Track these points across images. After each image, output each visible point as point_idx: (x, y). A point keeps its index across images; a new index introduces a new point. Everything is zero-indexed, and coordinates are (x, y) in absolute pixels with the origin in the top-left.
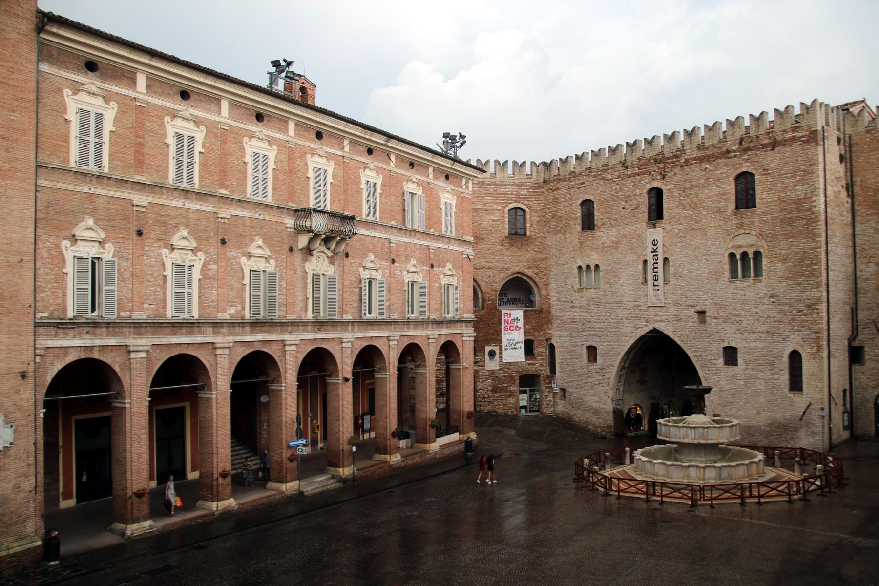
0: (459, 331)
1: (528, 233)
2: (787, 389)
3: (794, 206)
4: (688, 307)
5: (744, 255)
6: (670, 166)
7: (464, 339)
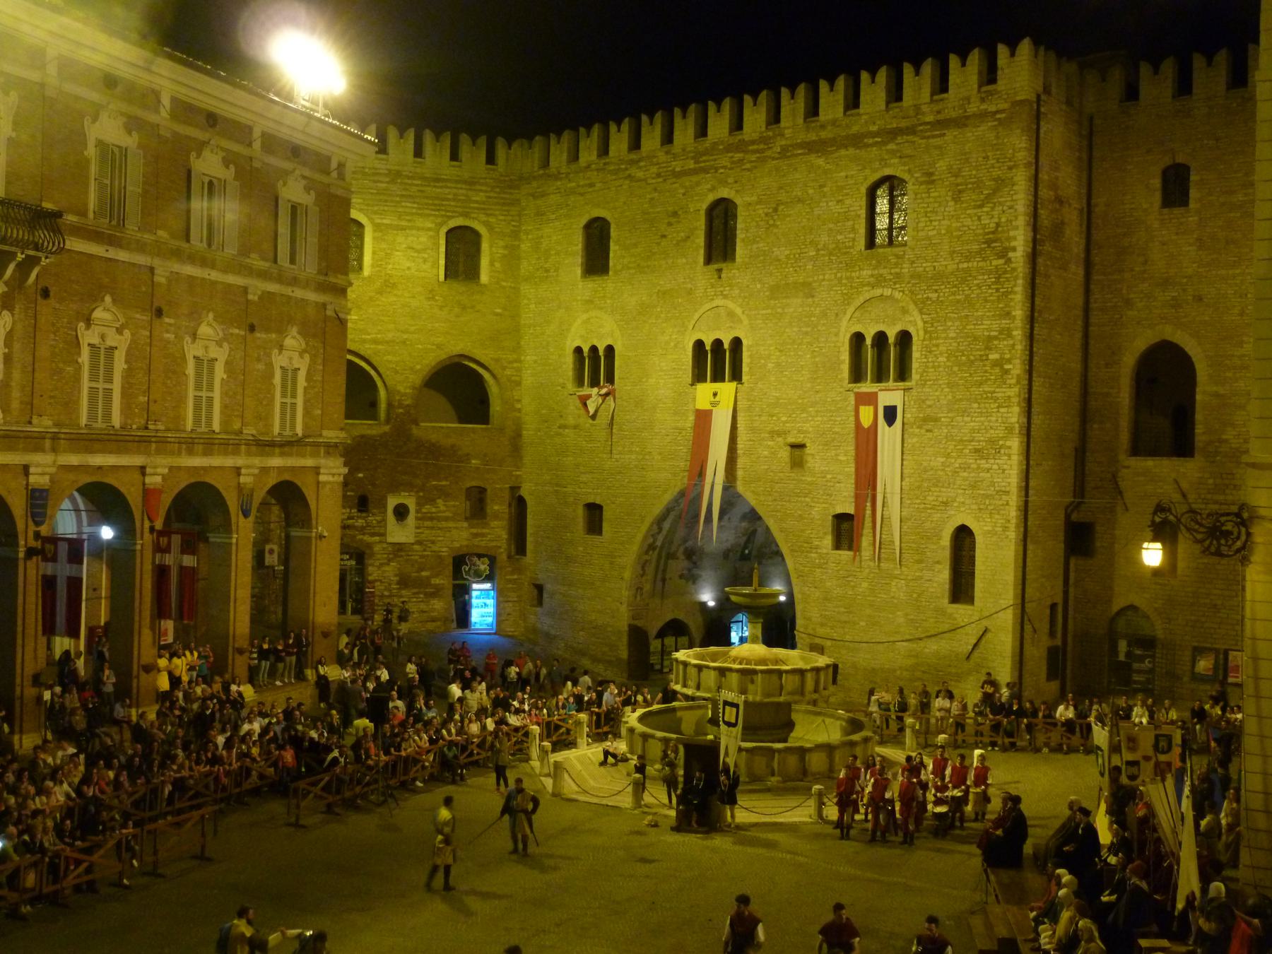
0: (309, 462)
1: (484, 278)
2: (946, 601)
3: (975, 247)
4: (774, 434)
5: (881, 338)
6: (753, 157)
7: (322, 478)
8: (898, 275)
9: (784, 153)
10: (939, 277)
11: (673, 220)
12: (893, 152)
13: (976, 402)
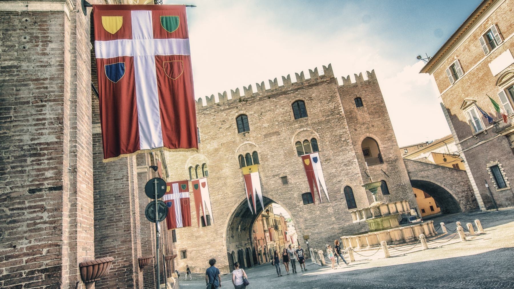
3: (329, 113)
4: (274, 176)
6: (250, 102)
8: (308, 124)
9: (261, 99)
10: (320, 123)
11: (223, 123)
12: (298, 94)
13: (341, 152)
